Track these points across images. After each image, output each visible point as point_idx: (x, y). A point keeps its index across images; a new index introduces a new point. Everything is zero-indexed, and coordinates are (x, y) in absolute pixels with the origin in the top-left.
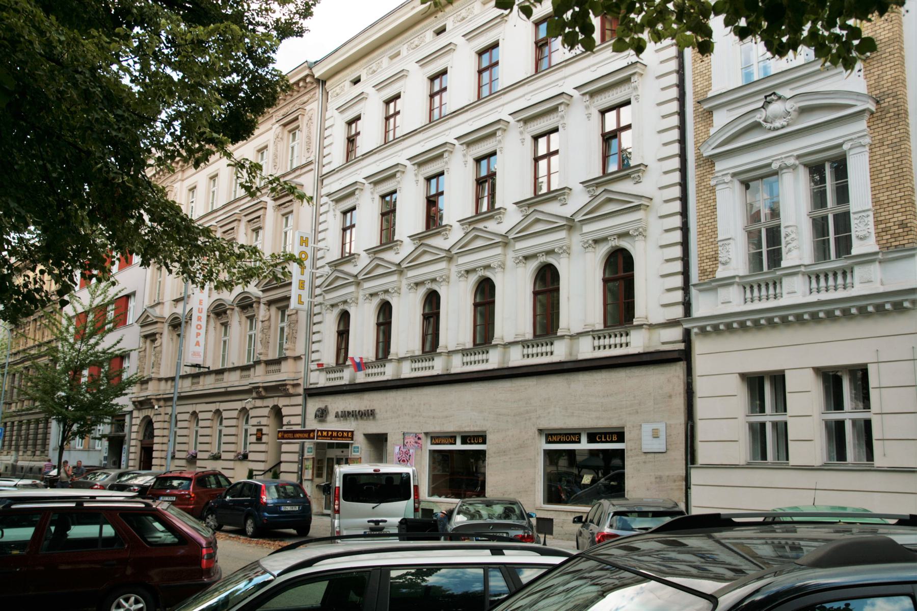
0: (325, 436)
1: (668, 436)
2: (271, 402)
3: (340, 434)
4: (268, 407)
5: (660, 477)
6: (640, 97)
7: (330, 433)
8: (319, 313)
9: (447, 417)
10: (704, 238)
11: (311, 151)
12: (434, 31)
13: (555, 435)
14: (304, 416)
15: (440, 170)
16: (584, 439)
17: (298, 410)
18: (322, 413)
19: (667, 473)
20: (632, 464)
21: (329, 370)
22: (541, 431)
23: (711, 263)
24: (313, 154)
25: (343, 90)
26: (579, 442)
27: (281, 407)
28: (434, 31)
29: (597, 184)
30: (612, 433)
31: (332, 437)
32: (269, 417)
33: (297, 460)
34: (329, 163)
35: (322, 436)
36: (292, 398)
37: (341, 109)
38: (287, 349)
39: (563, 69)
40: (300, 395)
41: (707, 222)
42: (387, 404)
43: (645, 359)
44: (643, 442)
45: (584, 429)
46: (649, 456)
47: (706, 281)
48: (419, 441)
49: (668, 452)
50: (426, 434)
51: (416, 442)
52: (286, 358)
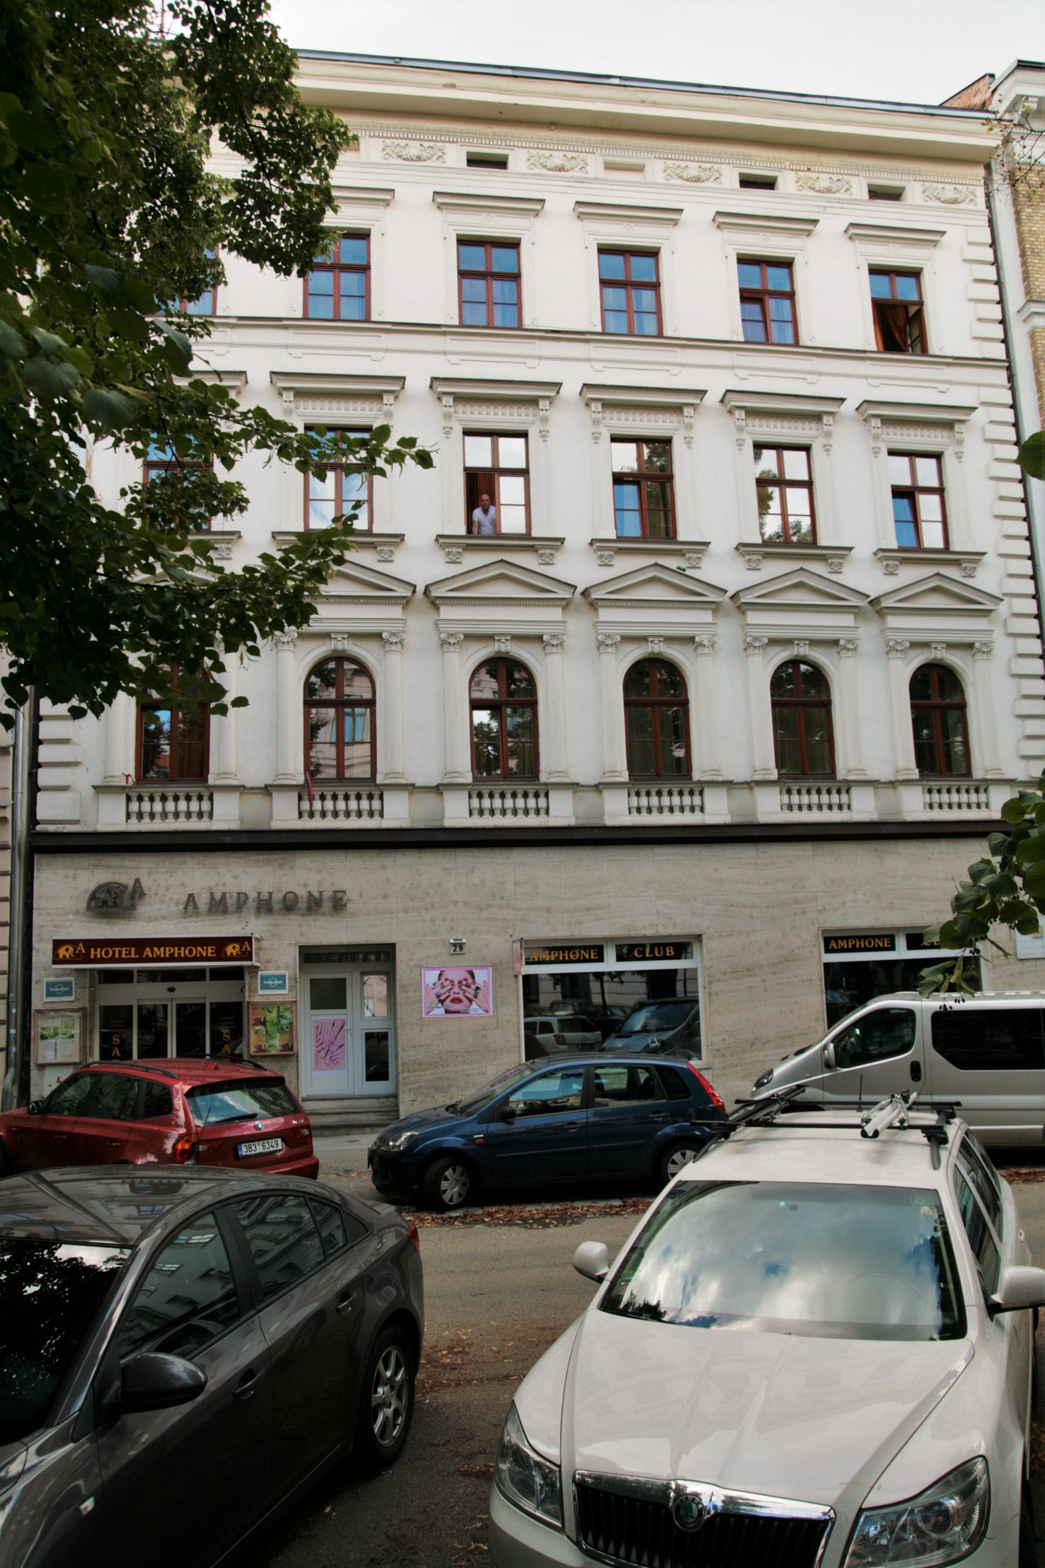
6: (964, 456)
13: (842, 938)
16: (901, 942)
30: (664, 945)
39: (815, 359)
42: (387, 880)
46: (1027, 964)
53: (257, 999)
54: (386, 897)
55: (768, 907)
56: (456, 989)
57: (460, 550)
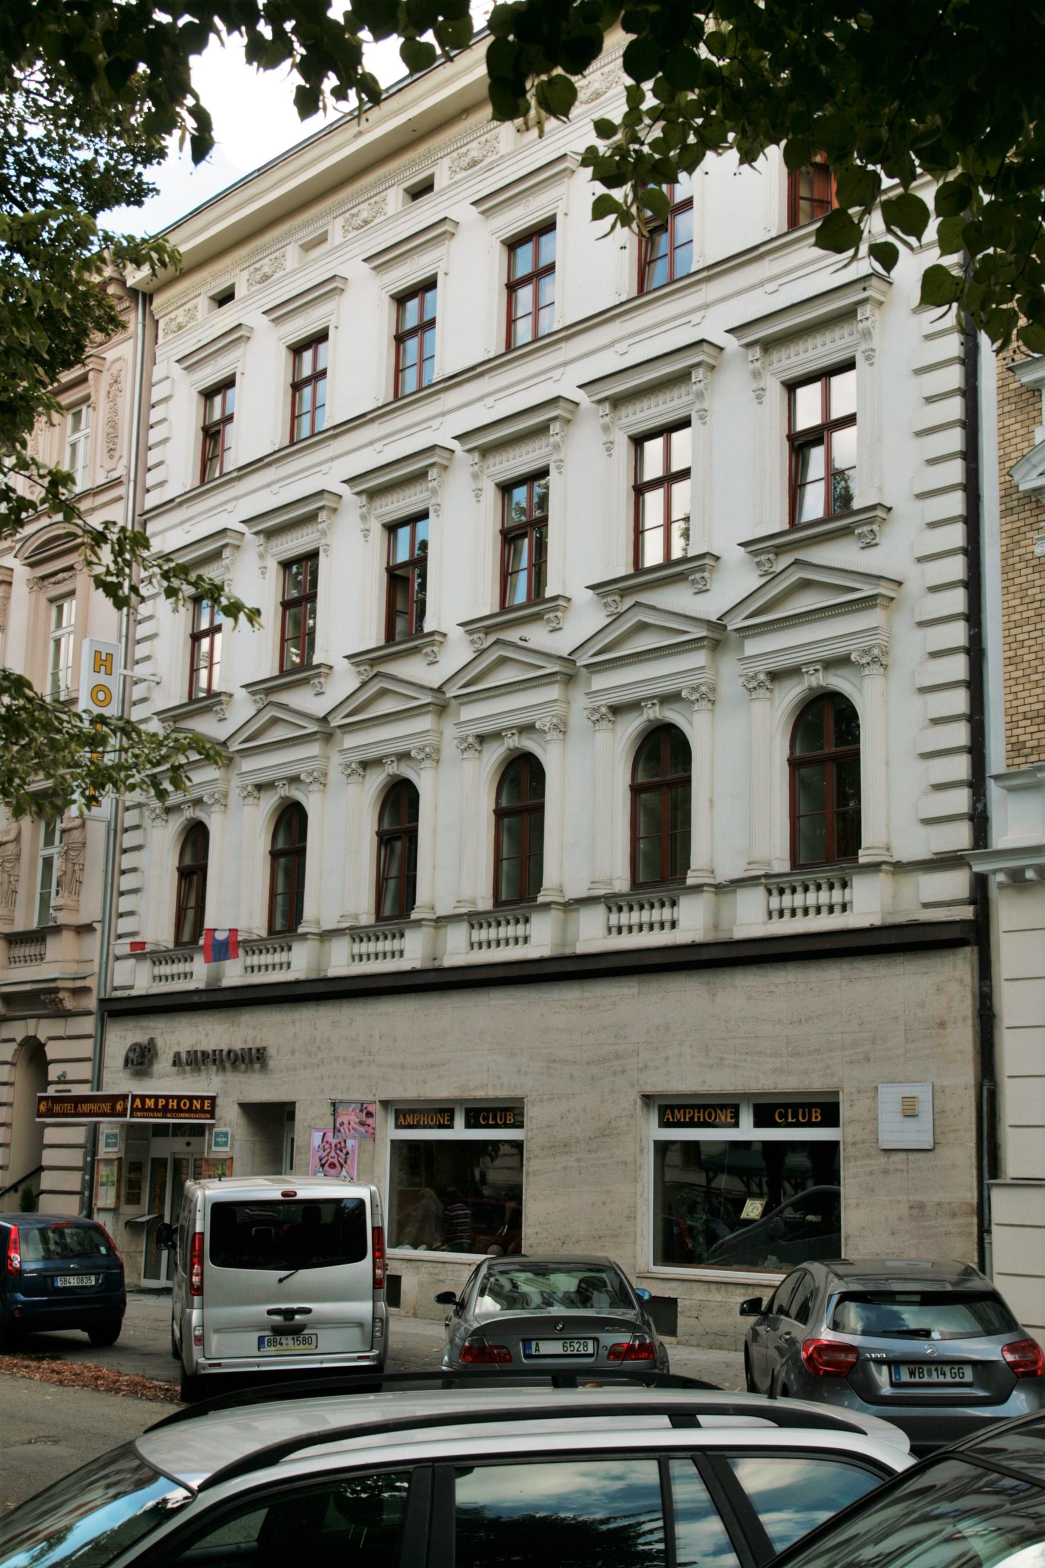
0: (149, 1110)
1: (937, 1114)
2: (19, 1030)
3: (185, 1105)
4: (13, 1040)
5: (921, 1206)
6: (877, 354)
7: (161, 1103)
8: (137, 827)
9: (433, 1066)
10: (1020, 673)
11: (117, 455)
12: (406, 190)
13: (680, 1107)
14: (98, 1061)
15: (419, 508)
16: (746, 1118)
17: (86, 1048)
18: (142, 1055)
19: (936, 1198)
20: (855, 1177)
21: (159, 957)
22: (648, 1099)
23: (1035, 728)
24: (124, 461)
25: (193, 318)
26: (736, 1125)
27: (43, 1040)
28: (406, 190)
29: (777, 547)
31: (165, 1111)
32: (13, 1064)
33: (80, 1164)
34: (161, 484)
35: (143, 1109)
36: (71, 1020)
37: (190, 362)
38: (59, 909)
40: (88, 1013)
41: (1026, 636)
43: (884, 939)
44: (882, 1127)
45: (746, 1096)
47: (1024, 767)
48: (370, 1121)
49: (938, 1150)
50: (385, 1104)
51: (362, 1124)
52: (57, 929)
53: (213, 1156)
54: (293, 1052)
55: (588, 1063)
56: (333, 1154)
57: (481, 635)
